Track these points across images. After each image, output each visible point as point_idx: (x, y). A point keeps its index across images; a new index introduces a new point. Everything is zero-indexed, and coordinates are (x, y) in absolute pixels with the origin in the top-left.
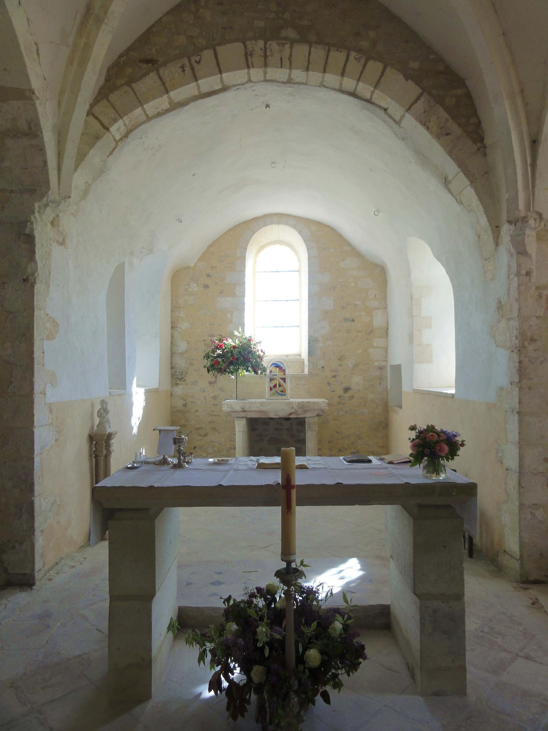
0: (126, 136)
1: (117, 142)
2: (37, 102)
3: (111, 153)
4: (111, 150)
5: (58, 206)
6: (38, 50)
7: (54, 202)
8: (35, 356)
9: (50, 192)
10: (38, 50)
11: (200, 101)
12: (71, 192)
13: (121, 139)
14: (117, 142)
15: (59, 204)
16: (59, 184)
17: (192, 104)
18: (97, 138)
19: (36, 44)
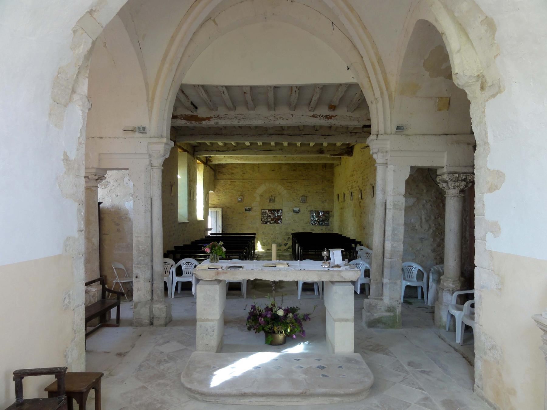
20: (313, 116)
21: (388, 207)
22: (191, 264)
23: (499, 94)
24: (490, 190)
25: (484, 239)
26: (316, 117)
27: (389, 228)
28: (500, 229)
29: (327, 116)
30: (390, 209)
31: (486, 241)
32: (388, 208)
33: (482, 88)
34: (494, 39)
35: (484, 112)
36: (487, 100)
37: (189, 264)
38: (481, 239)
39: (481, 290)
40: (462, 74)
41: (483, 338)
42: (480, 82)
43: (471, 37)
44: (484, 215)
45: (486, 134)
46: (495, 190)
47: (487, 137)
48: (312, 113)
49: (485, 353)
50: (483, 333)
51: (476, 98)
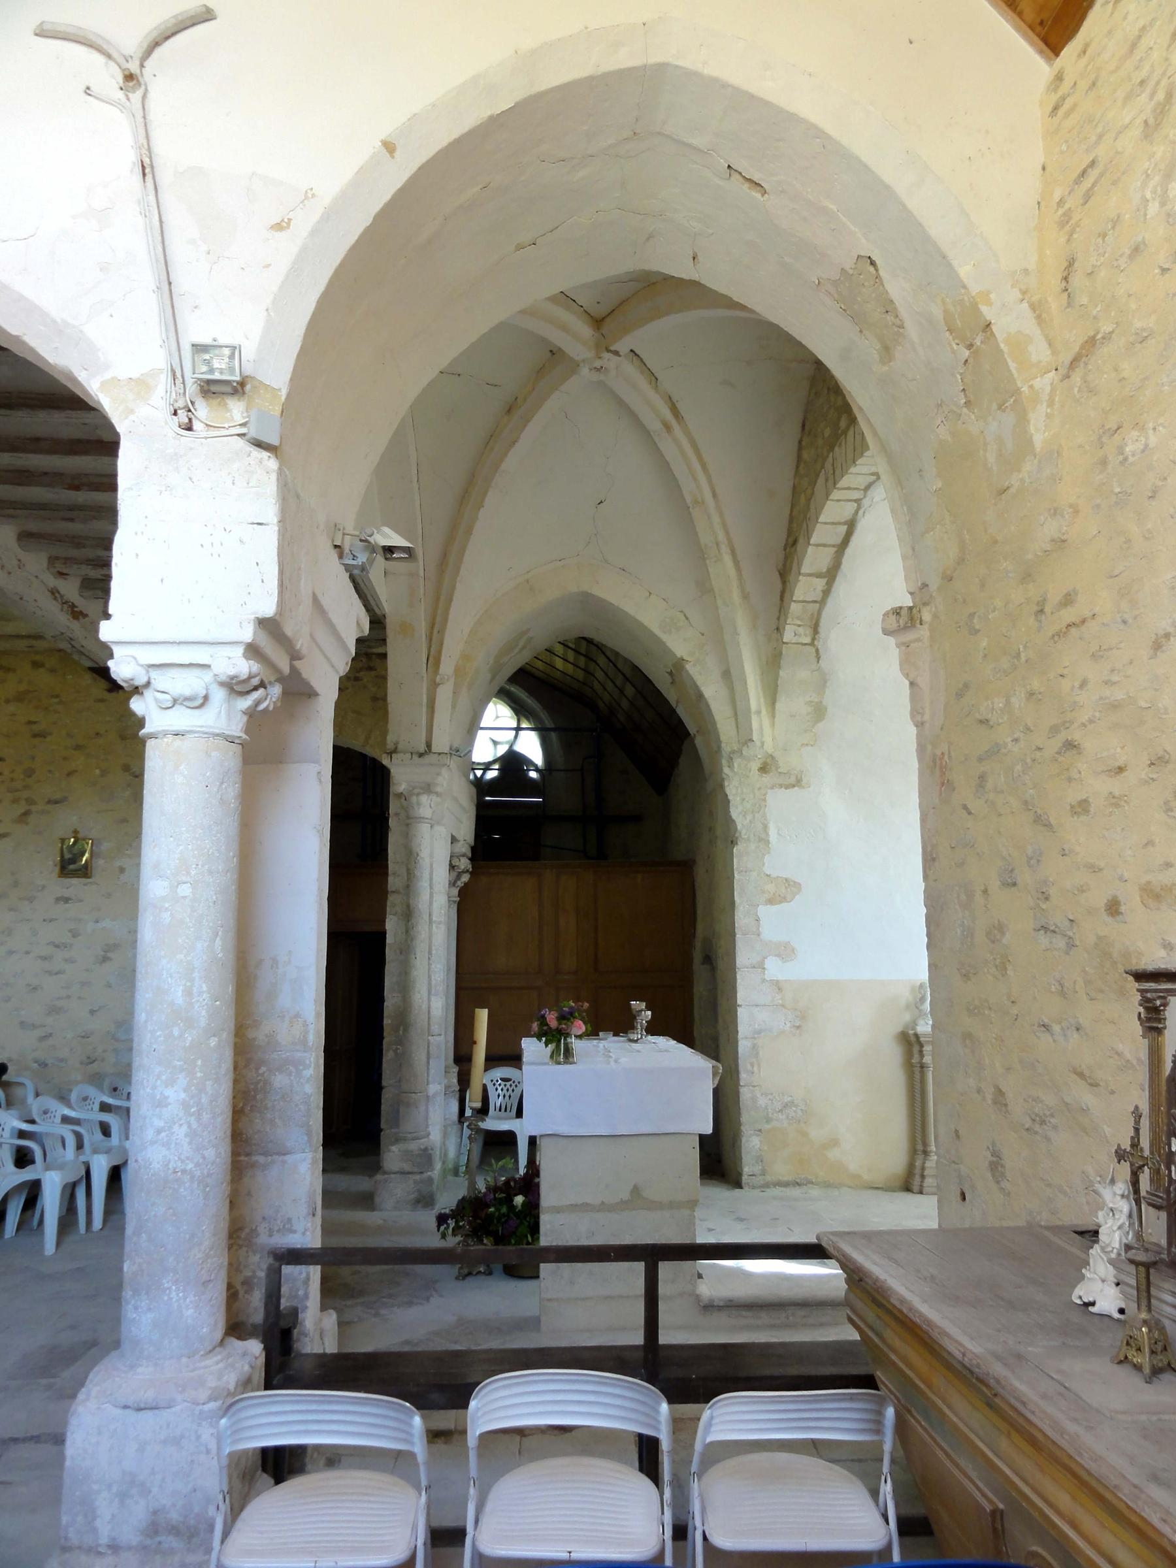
0: (815, 629)
1: (812, 644)
2: (688, 667)
3: (818, 658)
4: (815, 654)
5: (742, 753)
6: (685, 615)
7: (733, 752)
8: (736, 925)
9: (723, 745)
10: (685, 615)
11: (849, 551)
12: (752, 734)
13: (813, 639)
14: (812, 644)
15: (740, 751)
16: (738, 732)
17: (845, 560)
18: (781, 654)
19: (682, 612)
20: (54, 592)
21: (434, 919)
22: (513, 1085)
23: (796, 788)
24: (770, 902)
25: (761, 966)
26: (55, 599)
27: (439, 966)
28: (793, 950)
29: (73, 606)
30: (440, 923)
31: (764, 968)
32: (435, 922)
33: (764, 769)
34: (813, 726)
35: (765, 800)
36: (772, 788)
37: (508, 1084)
38: (754, 967)
39: (756, 1036)
40: (758, 743)
41: (762, 1101)
42: (761, 761)
43: (778, 705)
44: (759, 935)
45: (765, 828)
46: (781, 902)
47: (767, 834)
48: (53, 582)
49: (768, 1120)
50: (762, 1094)
51: (748, 777)
